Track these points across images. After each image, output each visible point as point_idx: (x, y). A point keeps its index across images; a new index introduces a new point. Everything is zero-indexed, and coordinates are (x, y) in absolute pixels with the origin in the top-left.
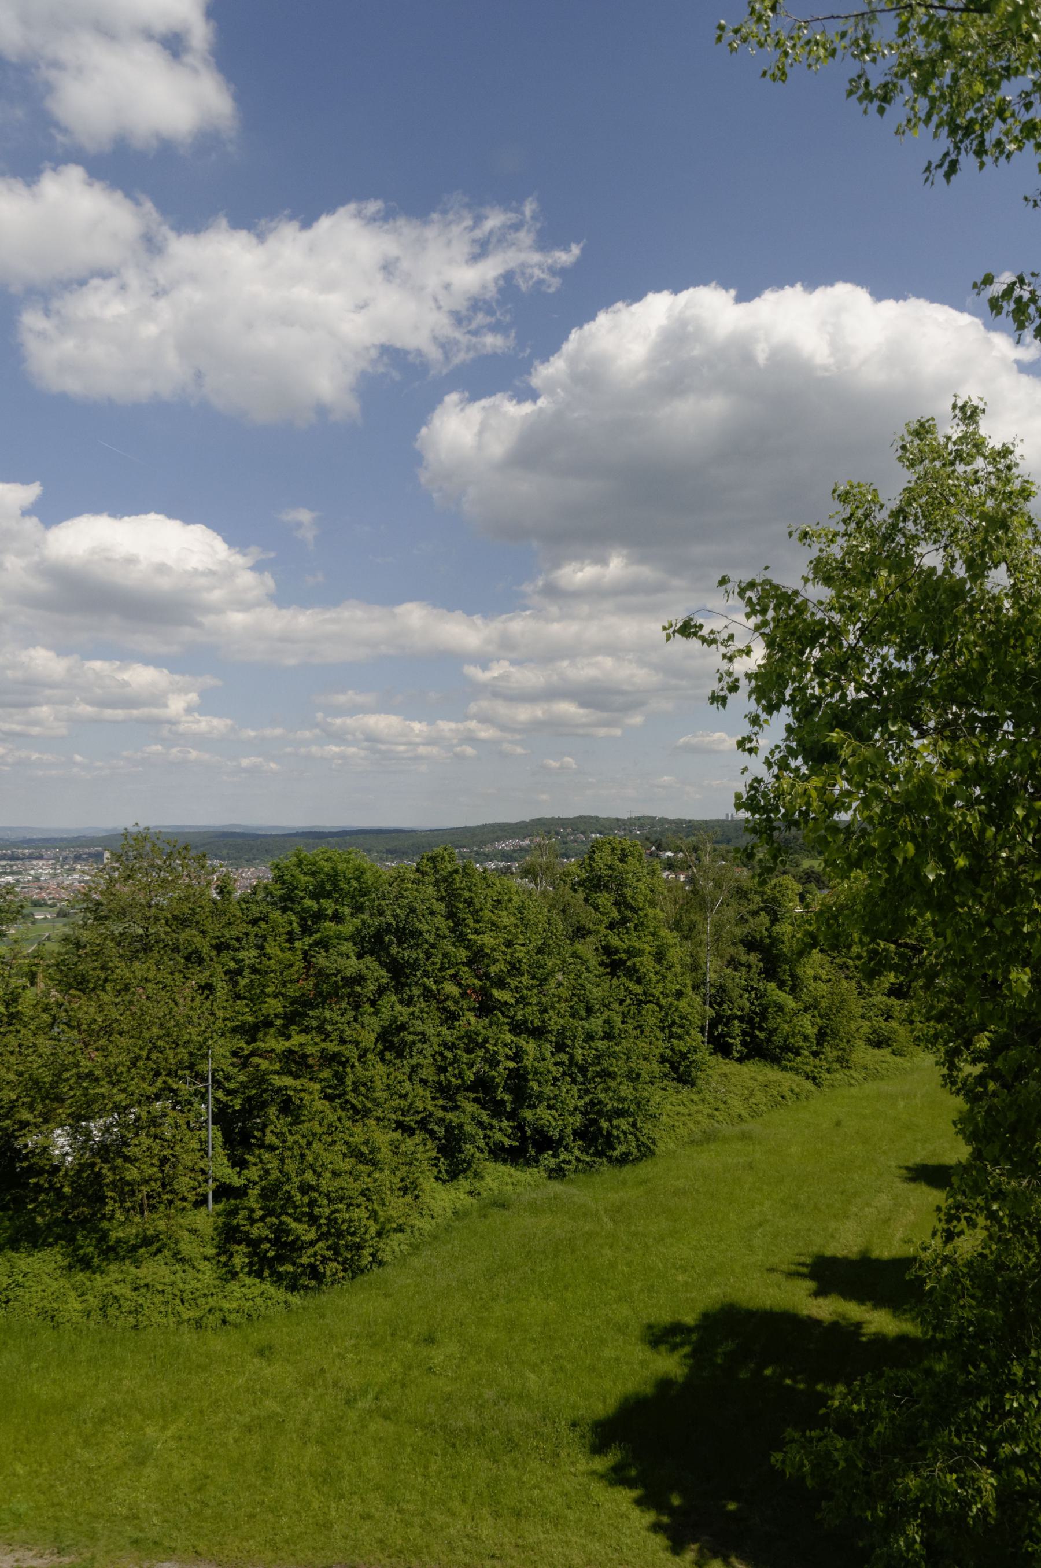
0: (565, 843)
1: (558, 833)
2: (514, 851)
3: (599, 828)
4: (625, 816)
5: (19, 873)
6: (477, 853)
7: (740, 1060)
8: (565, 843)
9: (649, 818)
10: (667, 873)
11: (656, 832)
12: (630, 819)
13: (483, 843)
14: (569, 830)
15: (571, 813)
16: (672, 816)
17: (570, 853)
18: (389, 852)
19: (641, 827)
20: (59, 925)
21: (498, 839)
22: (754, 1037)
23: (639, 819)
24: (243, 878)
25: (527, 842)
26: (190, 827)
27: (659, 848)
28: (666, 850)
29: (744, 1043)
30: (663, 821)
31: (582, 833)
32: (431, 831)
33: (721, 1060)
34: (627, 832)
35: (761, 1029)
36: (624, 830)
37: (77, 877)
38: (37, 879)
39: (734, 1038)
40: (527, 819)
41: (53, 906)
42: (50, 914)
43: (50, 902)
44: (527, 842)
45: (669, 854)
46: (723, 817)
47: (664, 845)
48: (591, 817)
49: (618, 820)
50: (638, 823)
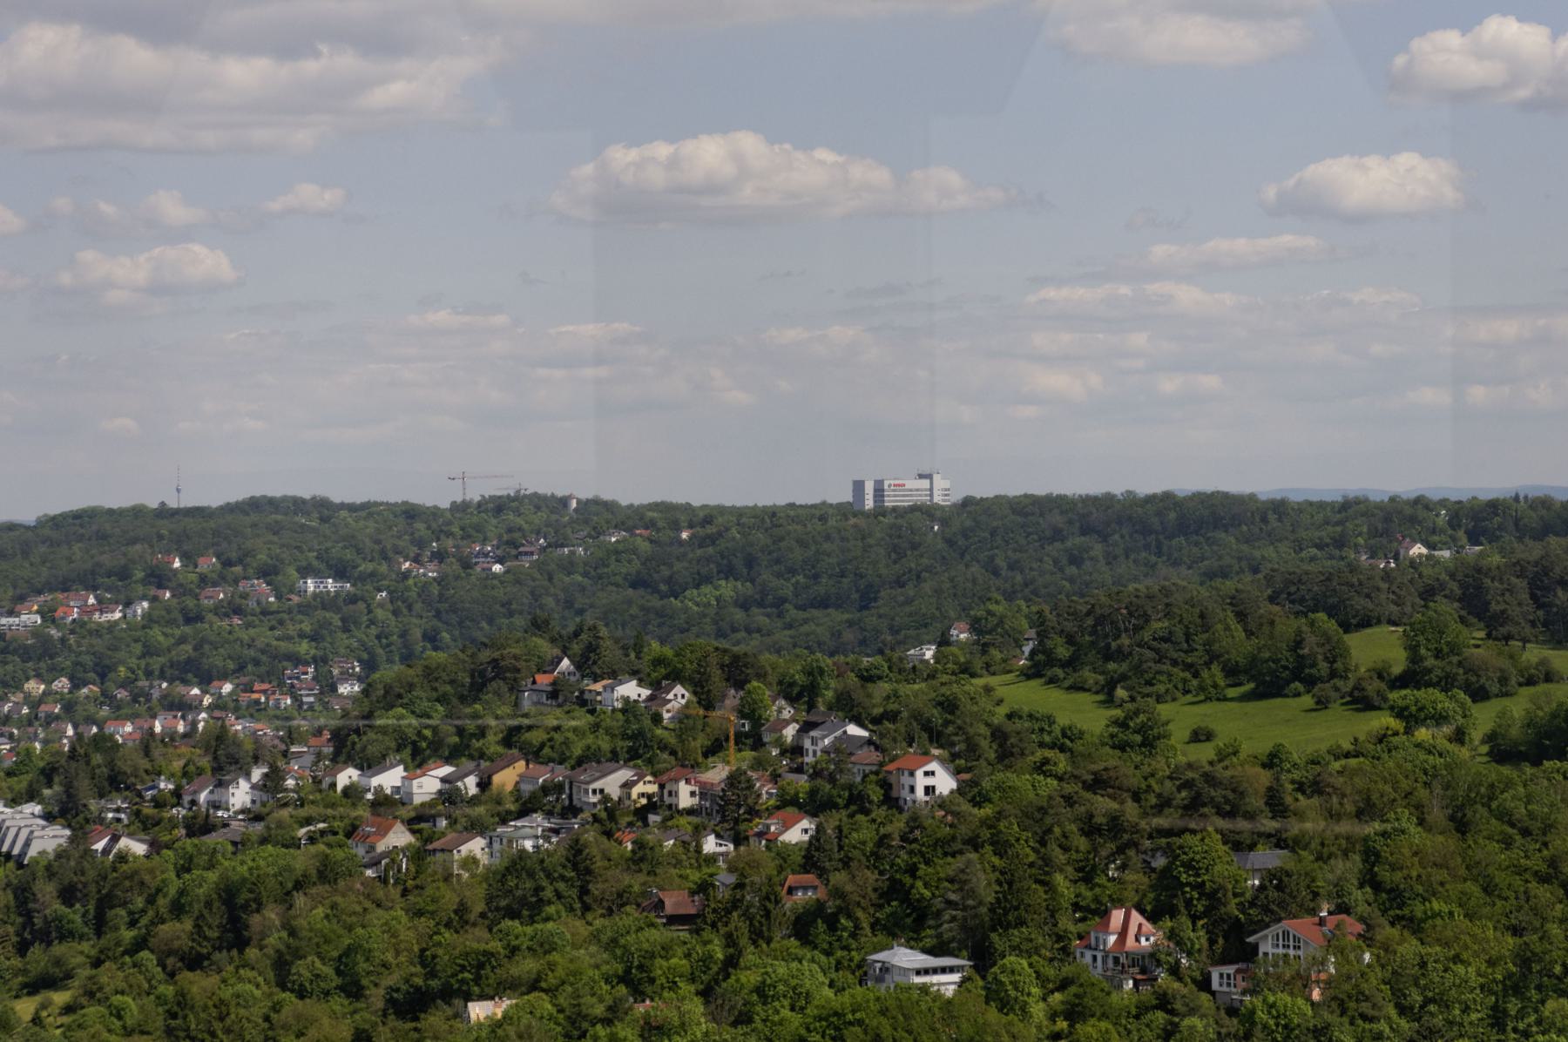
0: (192, 618)
1: (159, 578)
3: (336, 551)
4: (437, 495)
8: (192, 618)
9: (539, 502)
10: (624, 774)
11: (569, 566)
12: (460, 508)
14: (208, 563)
16: (631, 491)
17: (217, 660)
19: (510, 547)
23: (498, 506)
25: (29, 618)
27: (587, 664)
28: (615, 676)
30: (599, 514)
31: (266, 573)
34: (453, 566)
36: (439, 556)
44: (29, 618)
45: (631, 690)
46: (844, 495)
47: (610, 652)
48: (298, 505)
49: (410, 513)
50: (493, 526)
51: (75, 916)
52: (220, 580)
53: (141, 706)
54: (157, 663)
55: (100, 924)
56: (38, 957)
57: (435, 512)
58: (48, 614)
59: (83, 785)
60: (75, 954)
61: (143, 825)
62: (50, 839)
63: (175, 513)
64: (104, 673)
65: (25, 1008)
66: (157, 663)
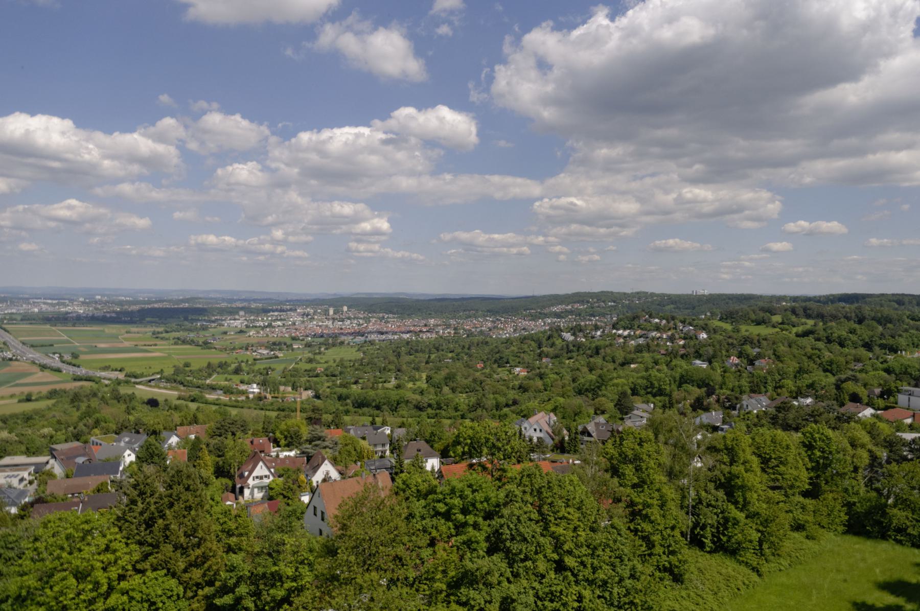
0: (592, 308)
1: (588, 302)
2: (562, 312)
4: (629, 291)
5: (284, 320)
6: (540, 313)
8: (592, 308)
9: (644, 292)
10: (655, 333)
11: (648, 302)
12: (632, 293)
13: (544, 307)
14: (595, 300)
15: (596, 289)
17: (596, 314)
18: (488, 311)
19: (639, 299)
20: (307, 352)
21: (553, 305)
23: (638, 293)
24: (405, 325)
25: (570, 307)
26: (377, 294)
27: (651, 316)
28: (654, 318)
30: (653, 295)
31: (604, 302)
32: (513, 298)
37: (315, 323)
38: (294, 324)
40: (570, 293)
41: (303, 340)
42: (302, 345)
43: (301, 338)
44: (570, 307)
45: (657, 320)
47: (654, 314)
48: (608, 292)
49: (625, 294)
51: (575, 349)
53: (585, 319)
55: (578, 351)
56: (569, 355)
58: (572, 307)
59: (576, 331)
60: (575, 354)
61: (585, 337)
62: (571, 338)
64: (580, 315)
65: (567, 362)
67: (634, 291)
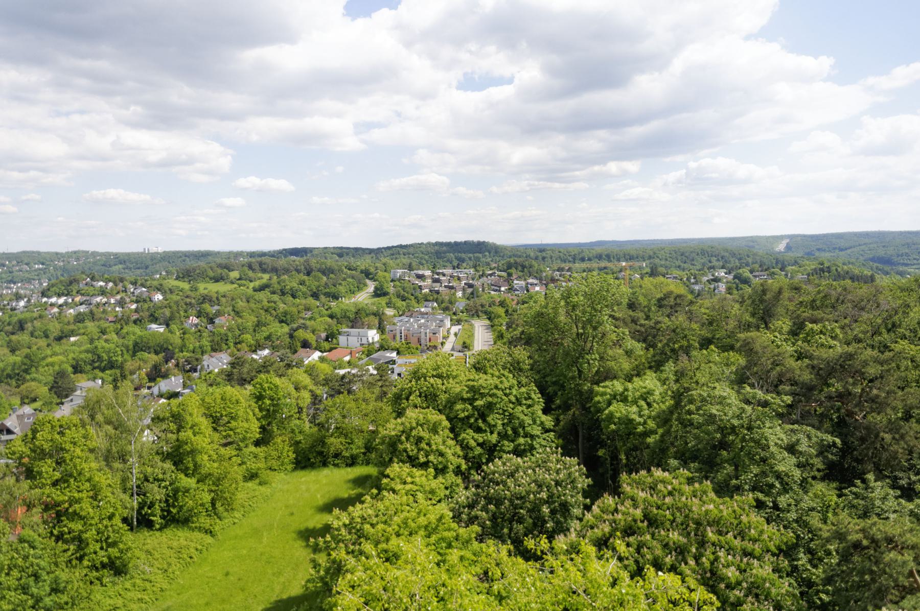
3: (41, 260)
4: (62, 249)
7: (160, 529)
9: (83, 252)
10: (101, 298)
11: (89, 262)
12: (68, 253)
14: (14, 262)
15: (15, 248)
16: (101, 249)
19: (78, 259)
22: (169, 512)
23: (75, 252)
27: (93, 279)
29: (163, 517)
30: (94, 254)
31: (27, 264)
33: (146, 533)
35: (174, 506)
36: (63, 261)
39: (155, 516)
45: (102, 283)
46: (142, 251)
47: (97, 277)
48: (33, 252)
49: (57, 254)
52: (17, 265)
54: (3, 280)
57: (62, 253)
63: (6, 254)
66: (3, 280)
67: (70, 250)
